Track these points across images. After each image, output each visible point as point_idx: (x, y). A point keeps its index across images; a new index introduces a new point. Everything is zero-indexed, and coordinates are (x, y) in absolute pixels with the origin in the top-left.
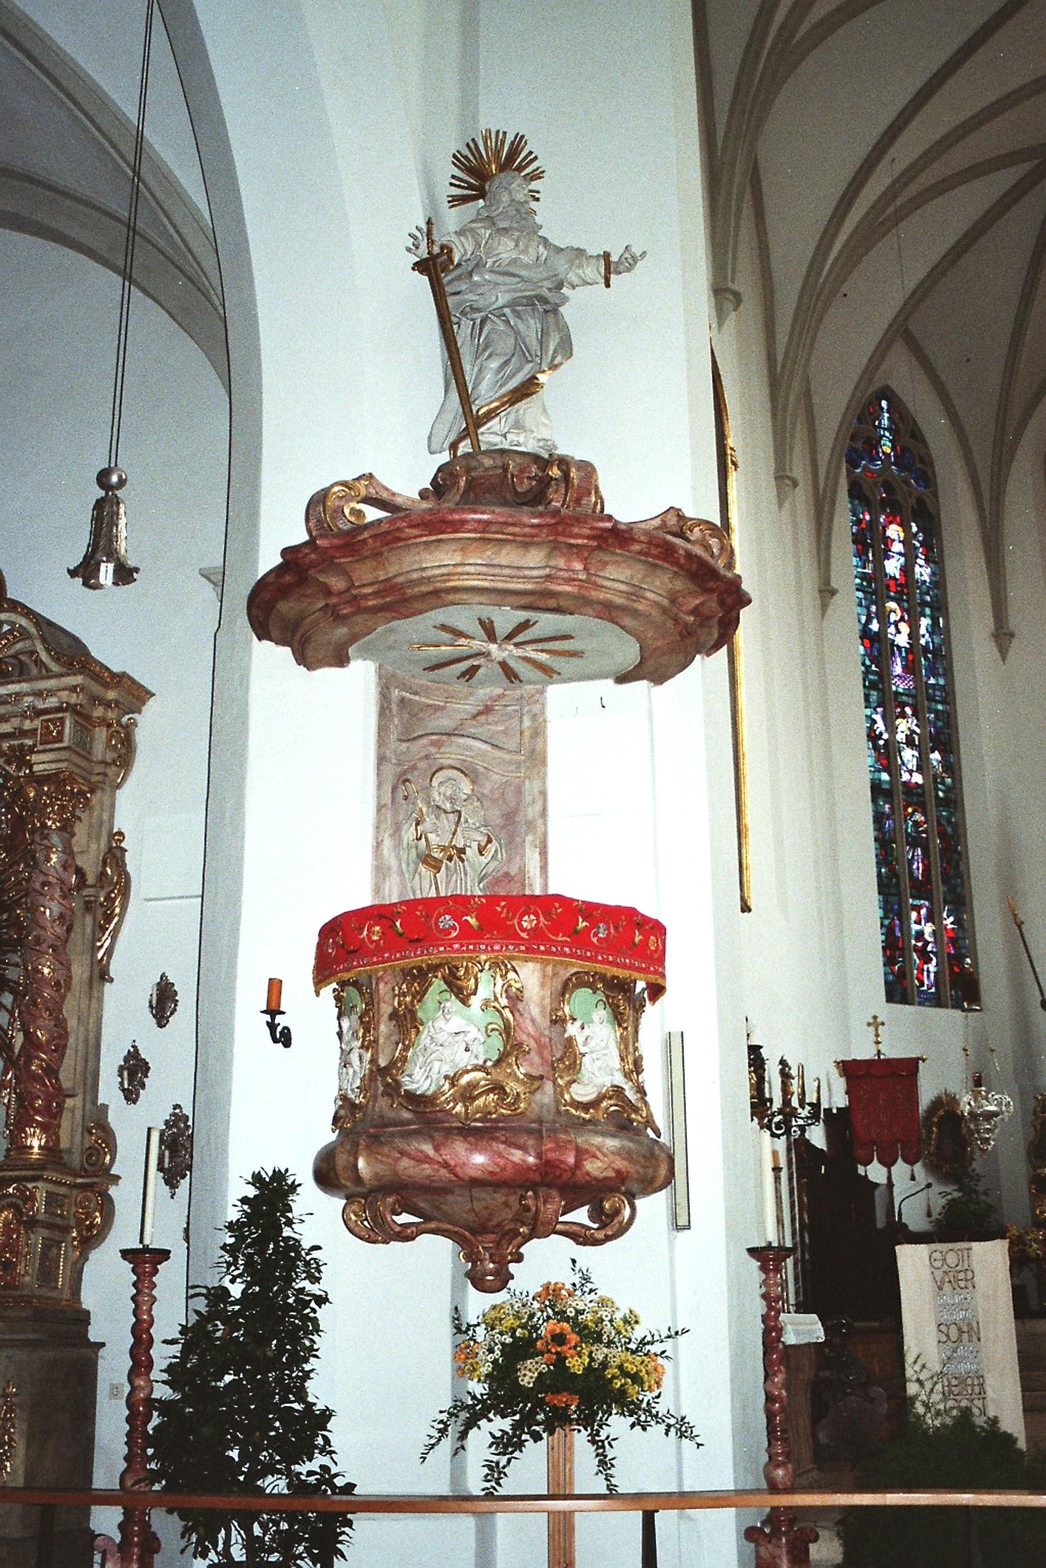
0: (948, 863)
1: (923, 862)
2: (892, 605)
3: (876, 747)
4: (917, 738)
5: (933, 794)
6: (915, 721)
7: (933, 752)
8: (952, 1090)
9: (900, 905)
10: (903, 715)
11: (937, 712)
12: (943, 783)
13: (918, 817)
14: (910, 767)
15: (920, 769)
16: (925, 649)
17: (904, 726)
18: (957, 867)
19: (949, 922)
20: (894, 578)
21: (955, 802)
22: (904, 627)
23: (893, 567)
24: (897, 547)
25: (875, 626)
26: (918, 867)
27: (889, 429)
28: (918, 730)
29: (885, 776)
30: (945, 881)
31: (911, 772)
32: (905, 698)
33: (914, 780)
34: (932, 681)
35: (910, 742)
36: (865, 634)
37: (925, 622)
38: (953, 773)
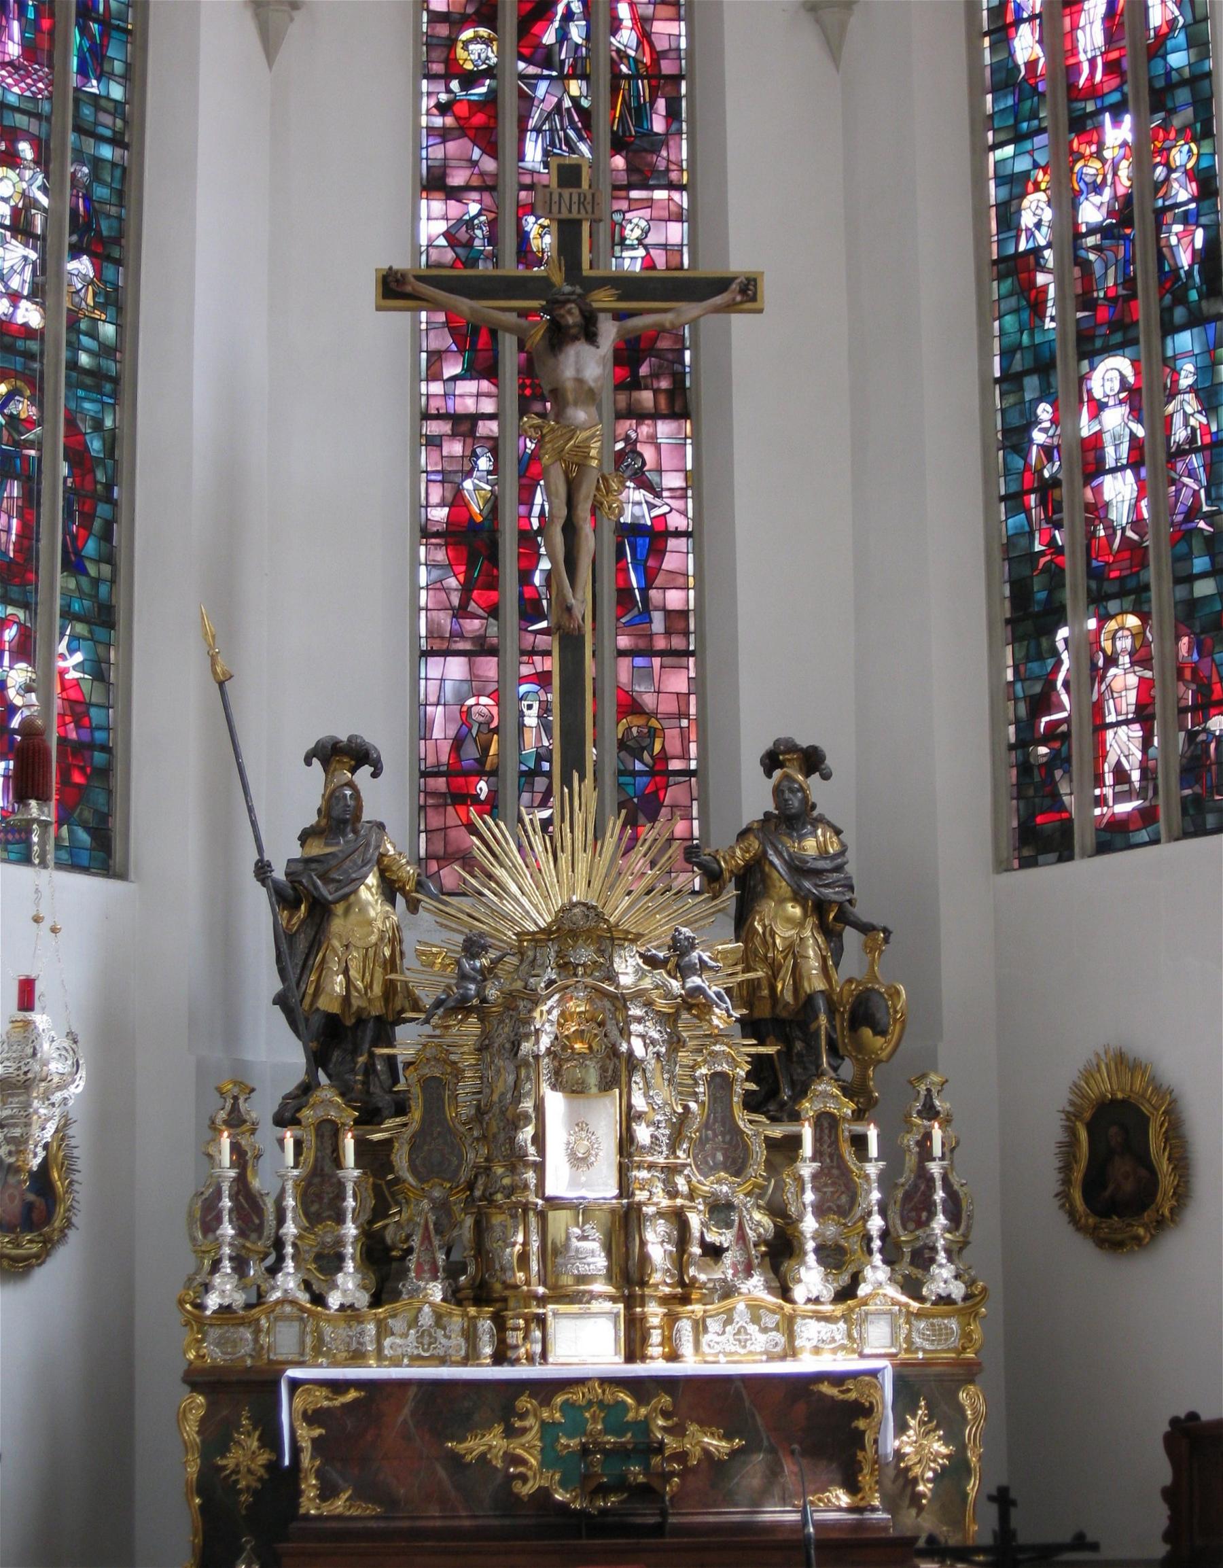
0: (86, 525)
1: (21, 517)
4: (38, 221)
5: (64, 354)
6: (40, 179)
7: (75, 252)
11: (96, 163)
12: (93, 334)
13: (23, 408)
14: (15, 284)
15: (37, 293)
18: (107, 536)
19: (71, 663)
21: (115, 380)
28: (44, 201)
30: (73, 563)
31: (14, 297)
32: (21, 120)
33: (20, 319)
34: (93, 87)
38: (120, 310)
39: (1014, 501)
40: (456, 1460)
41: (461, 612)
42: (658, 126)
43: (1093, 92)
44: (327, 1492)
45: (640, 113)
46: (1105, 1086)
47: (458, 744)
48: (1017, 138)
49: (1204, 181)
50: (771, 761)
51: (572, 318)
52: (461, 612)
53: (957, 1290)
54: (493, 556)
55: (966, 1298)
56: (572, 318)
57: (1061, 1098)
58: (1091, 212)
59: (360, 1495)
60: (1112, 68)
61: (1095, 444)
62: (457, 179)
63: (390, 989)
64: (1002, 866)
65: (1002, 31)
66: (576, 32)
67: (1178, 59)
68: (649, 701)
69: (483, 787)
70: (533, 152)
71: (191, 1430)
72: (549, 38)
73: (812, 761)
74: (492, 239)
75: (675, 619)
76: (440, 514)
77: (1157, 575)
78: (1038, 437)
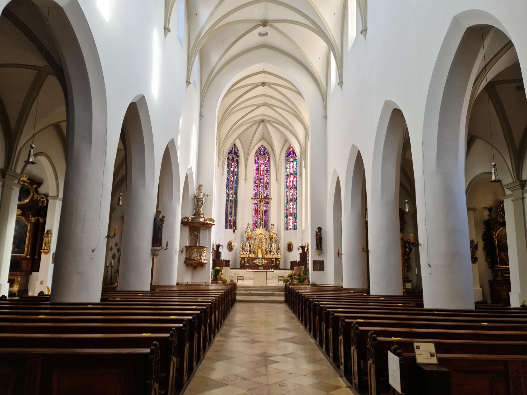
2: (232, 175)
3: (227, 195)
9: (228, 216)
10: (231, 190)
13: (232, 204)
15: (232, 198)
16: (235, 181)
17: (231, 192)
20: (232, 171)
22: (233, 178)
24: (233, 166)
25: (229, 178)
26: (231, 211)
27: (234, 149)
29: (228, 199)
35: (232, 194)
36: (228, 179)
37: (236, 177)
39: (286, 210)
40: (253, 262)
41: (255, 215)
42: (267, 186)
43: (291, 187)
45: (266, 186)
46: (289, 243)
47: (255, 222)
48: (287, 189)
50: (272, 225)
52: (255, 215)
53: (280, 254)
54: (257, 211)
55: (280, 255)
56: (261, 201)
57: (287, 244)
58: (291, 194)
59: (249, 264)
60: (292, 186)
61: (290, 207)
62: (256, 189)
63: (251, 237)
64: (284, 230)
65: (287, 183)
67: (296, 186)
71: (240, 260)
72: (261, 181)
73: (273, 225)
74: (258, 193)
75: (267, 215)
77: (293, 215)
78: (287, 206)
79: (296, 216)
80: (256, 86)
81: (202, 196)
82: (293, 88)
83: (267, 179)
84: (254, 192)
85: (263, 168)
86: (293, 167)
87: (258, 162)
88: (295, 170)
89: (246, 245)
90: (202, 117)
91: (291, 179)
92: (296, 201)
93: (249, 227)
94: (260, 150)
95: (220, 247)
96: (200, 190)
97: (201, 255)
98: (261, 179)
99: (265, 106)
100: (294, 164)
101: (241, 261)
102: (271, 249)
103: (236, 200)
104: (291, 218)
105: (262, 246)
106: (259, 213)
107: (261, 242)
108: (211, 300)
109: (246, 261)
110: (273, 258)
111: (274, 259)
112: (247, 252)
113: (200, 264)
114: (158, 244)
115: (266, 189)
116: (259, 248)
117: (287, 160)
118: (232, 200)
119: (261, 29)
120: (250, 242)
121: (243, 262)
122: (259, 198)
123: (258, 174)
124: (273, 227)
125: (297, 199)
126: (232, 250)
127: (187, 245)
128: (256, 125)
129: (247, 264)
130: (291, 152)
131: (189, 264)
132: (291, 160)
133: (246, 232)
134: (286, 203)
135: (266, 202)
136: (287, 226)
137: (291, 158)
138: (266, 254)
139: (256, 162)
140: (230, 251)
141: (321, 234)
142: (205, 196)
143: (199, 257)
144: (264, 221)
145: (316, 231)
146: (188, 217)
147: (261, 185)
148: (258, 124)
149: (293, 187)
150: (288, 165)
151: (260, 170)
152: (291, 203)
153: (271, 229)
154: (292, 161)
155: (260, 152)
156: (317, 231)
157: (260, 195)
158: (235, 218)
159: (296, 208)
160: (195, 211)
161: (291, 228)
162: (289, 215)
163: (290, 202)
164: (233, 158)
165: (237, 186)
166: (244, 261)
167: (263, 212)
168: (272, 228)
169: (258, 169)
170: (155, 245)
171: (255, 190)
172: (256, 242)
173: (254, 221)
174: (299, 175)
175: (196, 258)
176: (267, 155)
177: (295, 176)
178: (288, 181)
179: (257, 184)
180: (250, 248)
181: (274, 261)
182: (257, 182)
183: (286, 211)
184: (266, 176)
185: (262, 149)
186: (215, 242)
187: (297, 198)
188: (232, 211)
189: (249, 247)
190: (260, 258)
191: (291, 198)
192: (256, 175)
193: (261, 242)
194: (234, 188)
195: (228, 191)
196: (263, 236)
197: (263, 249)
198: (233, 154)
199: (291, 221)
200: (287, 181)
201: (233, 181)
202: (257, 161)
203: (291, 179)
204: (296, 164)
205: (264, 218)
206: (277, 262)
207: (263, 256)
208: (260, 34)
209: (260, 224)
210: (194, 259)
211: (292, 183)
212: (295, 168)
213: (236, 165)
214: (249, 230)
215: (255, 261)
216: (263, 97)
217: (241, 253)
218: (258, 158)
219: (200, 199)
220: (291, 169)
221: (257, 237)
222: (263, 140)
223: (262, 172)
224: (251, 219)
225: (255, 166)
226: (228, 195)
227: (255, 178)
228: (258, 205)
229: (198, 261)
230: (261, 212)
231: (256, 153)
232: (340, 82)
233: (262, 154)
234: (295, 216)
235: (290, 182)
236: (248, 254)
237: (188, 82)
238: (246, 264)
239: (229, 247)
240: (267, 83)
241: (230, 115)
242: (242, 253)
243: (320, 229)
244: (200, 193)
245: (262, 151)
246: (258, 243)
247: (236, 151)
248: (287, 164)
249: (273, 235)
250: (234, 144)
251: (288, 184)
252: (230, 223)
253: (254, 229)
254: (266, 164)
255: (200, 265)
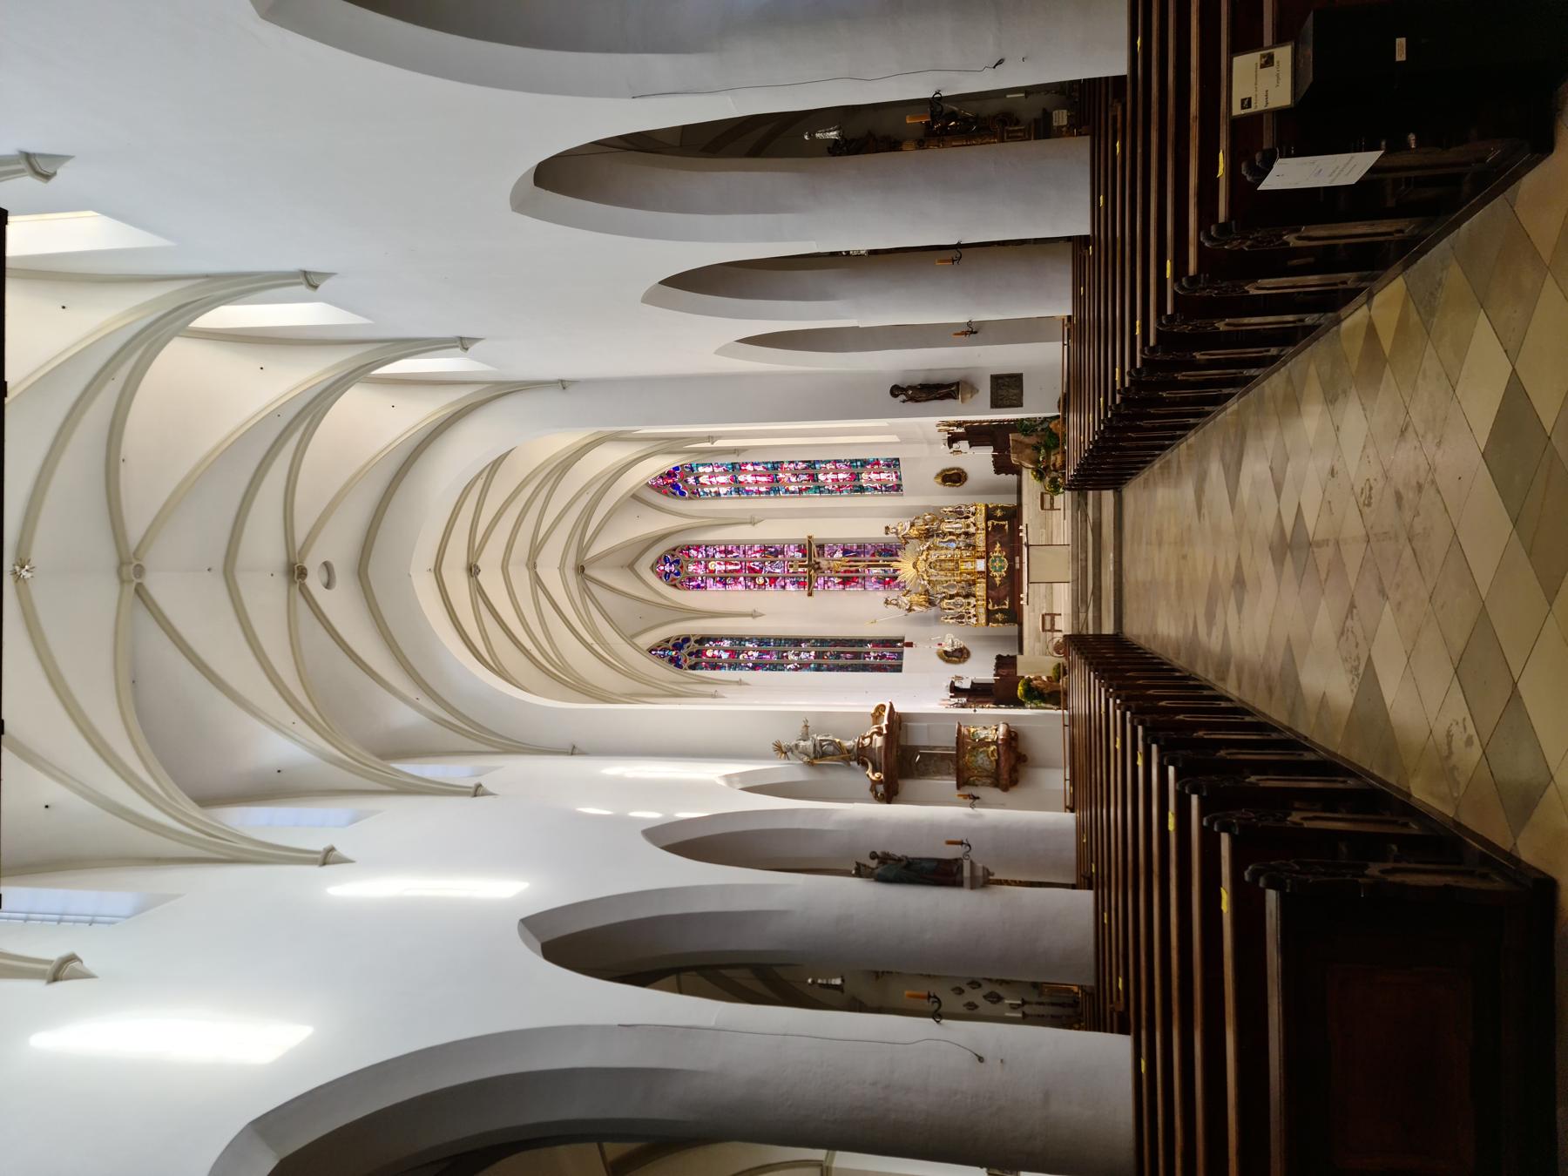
2: (741, 657)
3: (800, 668)
8: (935, 651)
10: (787, 657)
13: (828, 654)
17: (791, 657)
22: (750, 653)
23: (725, 656)
24: (716, 653)
25: (750, 665)
27: (665, 651)
29: (812, 666)
35: (798, 655)
36: (755, 667)
37: (747, 644)
41: (858, 583)
42: (773, 550)
43: (773, 479)
44: (1005, 604)
45: (771, 553)
46: (940, 480)
47: (880, 583)
49: (791, 462)
50: (887, 534)
51: (816, 566)
52: (858, 583)
56: (816, 566)
57: (942, 487)
58: (793, 479)
60: (769, 476)
61: (833, 480)
62: (783, 584)
63: (925, 595)
65: (760, 492)
66: (757, 564)
67: (769, 466)
68: (872, 552)
69: (887, 579)
70: (778, 571)
72: (758, 568)
73: (887, 528)
75: (859, 547)
76: (841, 586)
79: (859, 460)
80: (478, 591)
81: (809, 743)
82: (480, 483)
83: (750, 552)
84: (790, 588)
85: (719, 564)
86: (713, 474)
87: (702, 581)
88: (721, 469)
89: (950, 609)
90: (574, 747)
91: (750, 478)
92: (815, 462)
93: (894, 602)
94: (667, 575)
95: (957, 684)
96: (790, 749)
97: (984, 743)
98: (752, 570)
99: (535, 563)
100: (705, 473)
101: (997, 621)
102: (960, 534)
103: (817, 640)
104: (864, 476)
105: (952, 561)
106: (852, 572)
107: (938, 564)
108: (1118, 712)
109: (996, 608)
110: (987, 527)
111: (990, 523)
112: (969, 604)
113: (1010, 744)
114: (955, 869)
115: (782, 552)
116: (957, 568)
117: (693, 493)
118: (816, 652)
119: (314, 582)
120: (939, 596)
121: (999, 616)
122: (807, 575)
123: (736, 579)
124: (894, 530)
125: (810, 462)
126: (965, 648)
127: (955, 782)
128: (593, 588)
129: (1005, 604)
130: (669, 481)
131: (1010, 777)
132: (691, 480)
133: (910, 610)
134: (821, 492)
135: (818, 554)
136: (888, 489)
137: (686, 481)
138: (974, 547)
139: (703, 585)
140: (968, 654)
141: (910, 387)
142: (807, 734)
143: (989, 747)
144: (877, 558)
145: (904, 401)
146: (870, 784)
147: (768, 569)
148: (588, 583)
149: (774, 472)
150: (706, 490)
151: (725, 571)
152: (821, 477)
153: (900, 536)
154: (697, 479)
155: (672, 575)
156: (903, 397)
157: (800, 570)
158: (870, 642)
159: (836, 462)
160: (851, 763)
161: (894, 476)
162: (856, 483)
163: (818, 479)
164: (690, 654)
165: (775, 640)
166: (997, 612)
167: (849, 561)
168: (897, 533)
169: (721, 578)
170: (958, 877)
171: (784, 587)
172: (938, 578)
173: (878, 586)
174: (735, 456)
175: (993, 755)
176: (682, 552)
177: (741, 469)
178: (756, 488)
179: (765, 581)
180: (958, 595)
181: (996, 523)
182: (761, 581)
183: (845, 493)
184: (742, 555)
185: (662, 568)
186: (944, 700)
187: (804, 462)
188: (849, 653)
189: (956, 598)
190: (987, 567)
191: (805, 477)
192: (740, 583)
193: (938, 564)
194: (781, 648)
195: (791, 666)
196: (920, 558)
197: (961, 558)
198: (679, 654)
199: (873, 476)
200: (756, 493)
201: (760, 652)
202: (699, 582)
203: (750, 478)
204: (704, 465)
205: (868, 557)
206: (999, 513)
207: (982, 557)
208: (328, 586)
209: (886, 568)
210: (994, 763)
211: (760, 476)
212: (716, 470)
213: (711, 643)
214: (905, 599)
215: (998, 580)
216: (511, 568)
217: (975, 622)
218: (691, 579)
219: (818, 748)
220: (718, 482)
221: (925, 577)
222: (636, 567)
223: (730, 567)
224: (872, 594)
225: (714, 588)
226: (803, 666)
227: (749, 587)
228: (830, 575)
229: (1001, 751)
230: (850, 566)
231: (675, 586)
232: (458, 343)
233: (678, 568)
234: (859, 463)
235: (757, 482)
236: (977, 601)
237: (477, 791)
238: (1007, 607)
239: (957, 657)
240: (468, 561)
241: (565, 667)
242: (973, 620)
243: (896, 391)
244: (800, 749)
245: (667, 569)
246: (942, 573)
247: (670, 645)
248: (704, 492)
249: (918, 530)
250: (650, 652)
251: (763, 489)
252: (883, 657)
253: (902, 585)
254: (707, 556)
255: (1013, 744)
